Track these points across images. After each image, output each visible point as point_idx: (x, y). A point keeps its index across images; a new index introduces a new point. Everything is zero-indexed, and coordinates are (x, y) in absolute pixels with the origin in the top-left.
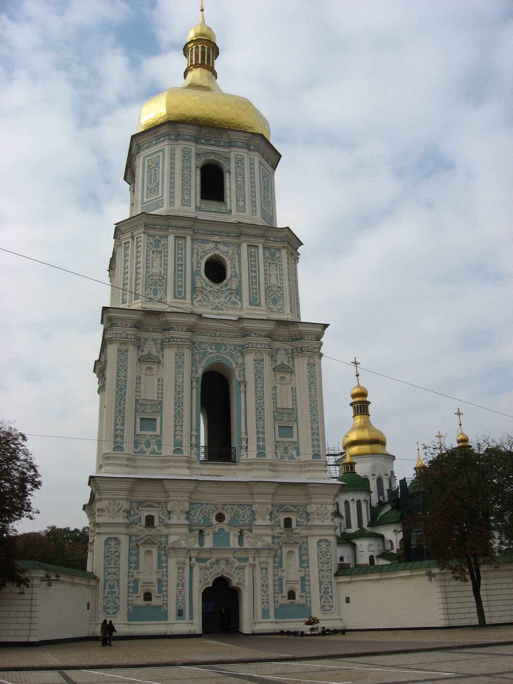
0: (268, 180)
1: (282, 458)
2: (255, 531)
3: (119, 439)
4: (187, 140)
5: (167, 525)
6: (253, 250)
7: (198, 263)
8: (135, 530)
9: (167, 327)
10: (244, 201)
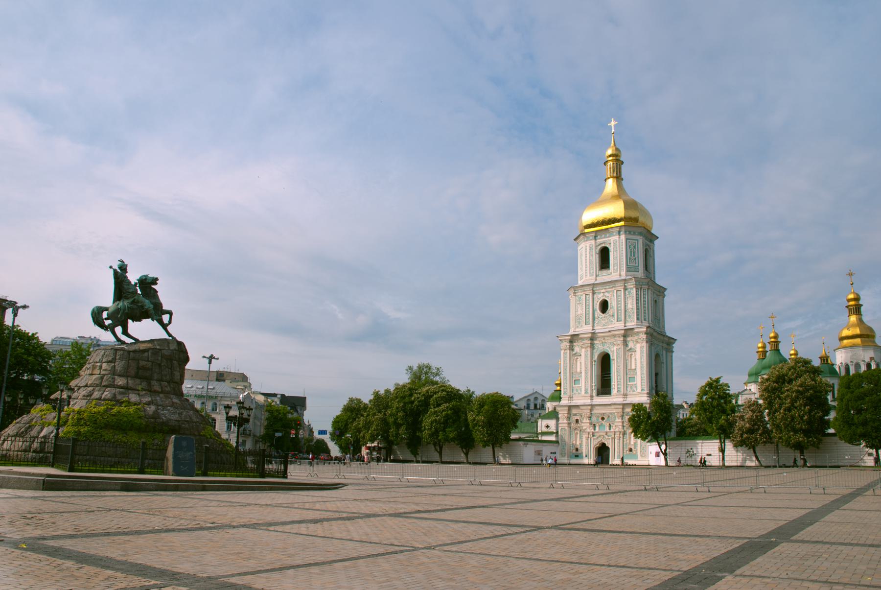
0: (635, 247)
1: (630, 392)
2: (615, 424)
3: (565, 390)
4: (591, 240)
5: (582, 423)
6: (619, 293)
7: (596, 305)
8: (572, 425)
9: (582, 339)
10: (617, 266)
